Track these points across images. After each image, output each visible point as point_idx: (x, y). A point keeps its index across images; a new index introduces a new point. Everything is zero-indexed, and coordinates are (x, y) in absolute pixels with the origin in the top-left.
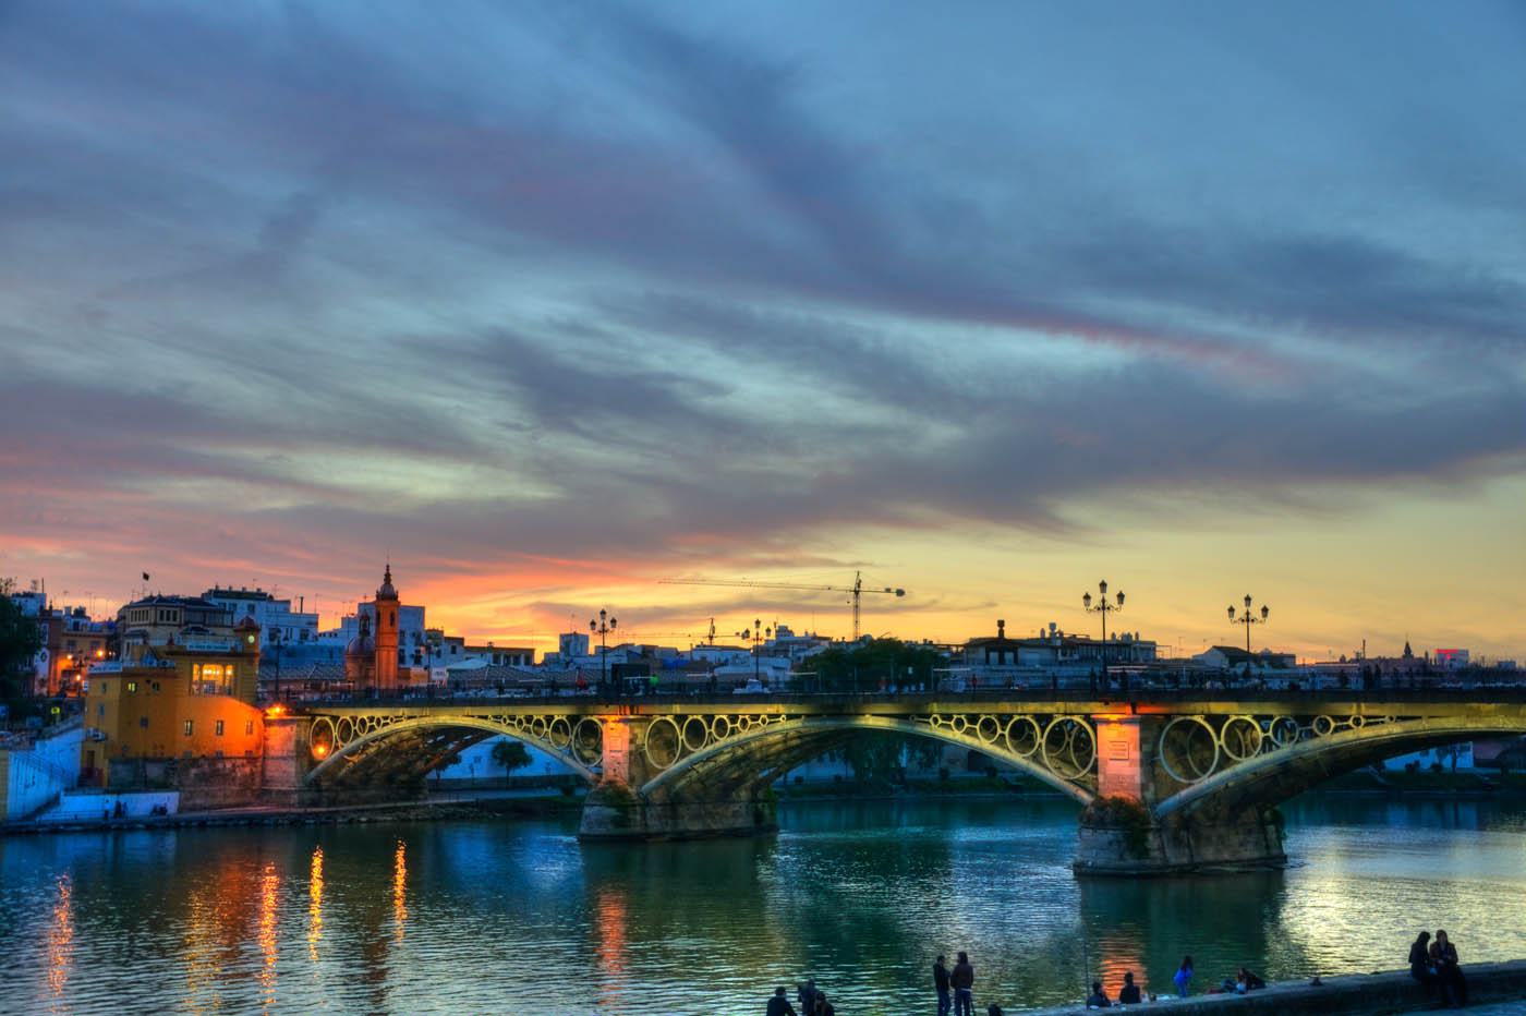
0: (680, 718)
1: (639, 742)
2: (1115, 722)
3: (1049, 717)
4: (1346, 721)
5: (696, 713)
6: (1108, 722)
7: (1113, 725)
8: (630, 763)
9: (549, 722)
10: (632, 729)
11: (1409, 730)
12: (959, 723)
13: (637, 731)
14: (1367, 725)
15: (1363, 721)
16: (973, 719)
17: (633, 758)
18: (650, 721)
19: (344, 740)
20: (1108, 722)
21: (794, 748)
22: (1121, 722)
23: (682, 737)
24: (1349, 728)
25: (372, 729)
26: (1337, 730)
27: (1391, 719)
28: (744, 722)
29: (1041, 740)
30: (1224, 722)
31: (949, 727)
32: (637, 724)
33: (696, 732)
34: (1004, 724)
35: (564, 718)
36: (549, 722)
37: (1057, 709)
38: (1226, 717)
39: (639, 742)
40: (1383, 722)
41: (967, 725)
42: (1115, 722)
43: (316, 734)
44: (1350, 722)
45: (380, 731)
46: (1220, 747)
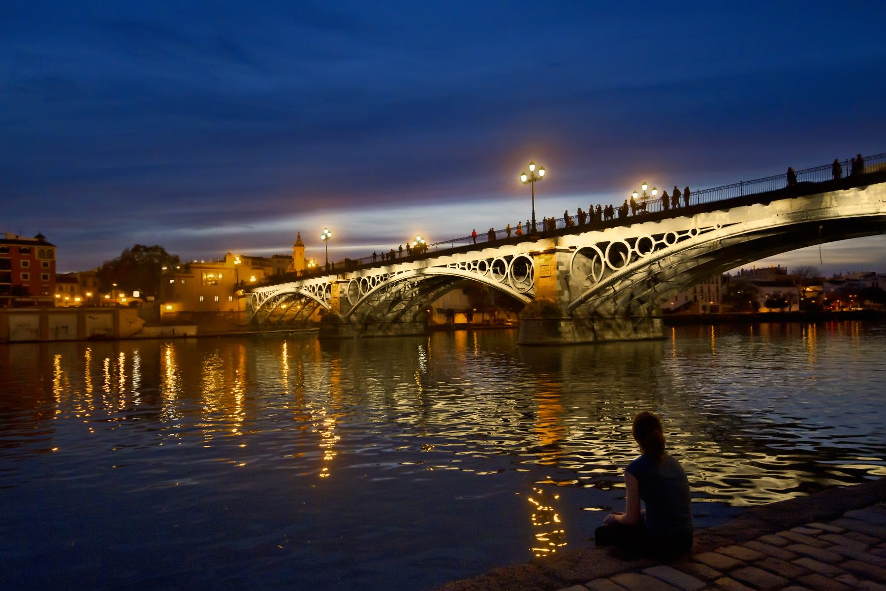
1: (345, 293)
2: (543, 253)
3: (511, 257)
4: (687, 233)
7: (542, 255)
8: (340, 303)
10: (341, 286)
11: (732, 232)
13: (344, 287)
14: (702, 233)
15: (699, 231)
17: (342, 300)
18: (349, 282)
19: (374, 285)
24: (688, 237)
26: (680, 240)
27: (719, 227)
29: (508, 269)
30: (635, 242)
32: (344, 284)
35: (355, 280)
38: (609, 242)
39: (345, 293)
40: (713, 230)
42: (543, 253)
44: (689, 234)
46: (605, 262)
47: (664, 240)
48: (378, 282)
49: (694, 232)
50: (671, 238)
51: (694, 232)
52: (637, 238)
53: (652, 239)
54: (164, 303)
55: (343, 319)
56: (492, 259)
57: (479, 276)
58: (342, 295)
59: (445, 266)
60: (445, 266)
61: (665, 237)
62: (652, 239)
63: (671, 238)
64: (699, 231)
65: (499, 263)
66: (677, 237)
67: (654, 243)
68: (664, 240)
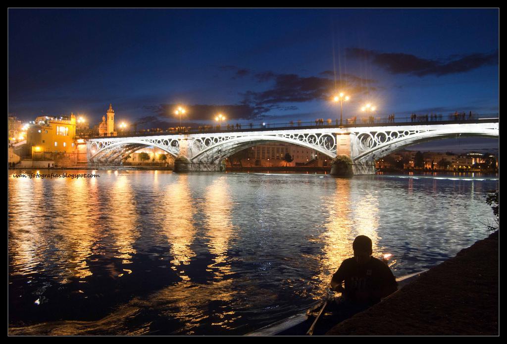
0: (203, 139)
3: (321, 134)
5: (208, 136)
6: (340, 134)
9: (162, 141)
12: (292, 137)
15: (419, 132)
16: (296, 135)
20: (340, 134)
21: (235, 148)
22: (345, 134)
23: (204, 143)
25: (109, 144)
26: (411, 134)
28: (223, 139)
29: (318, 140)
31: (288, 138)
33: (207, 142)
34: (306, 137)
36: (162, 141)
37: (324, 131)
38: (376, 132)
39: (190, 145)
41: (294, 137)
43: (92, 147)
44: (415, 132)
45: (111, 145)
47: (404, 134)
48: (220, 141)
49: (417, 132)
50: (407, 133)
51: (417, 132)
52: (376, 132)
53: (398, 133)
54: (34, 145)
55: (189, 161)
56: (308, 134)
57: (297, 142)
58: (188, 147)
59: (275, 135)
60: (275, 135)
61: (404, 132)
62: (398, 133)
63: (407, 133)
64: (419, 132)
65: (312, 136)
66: (410, 133)
67: (399, 134)
68: (404, 134)
